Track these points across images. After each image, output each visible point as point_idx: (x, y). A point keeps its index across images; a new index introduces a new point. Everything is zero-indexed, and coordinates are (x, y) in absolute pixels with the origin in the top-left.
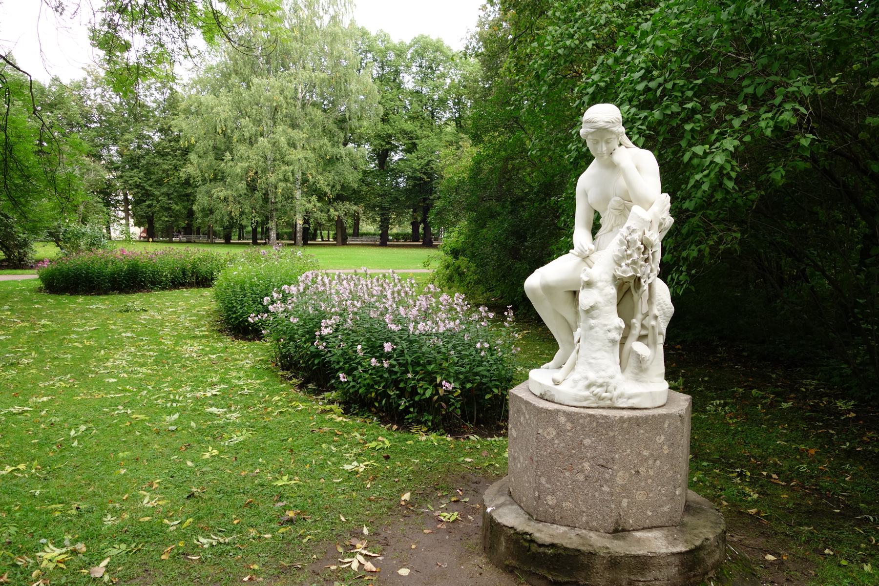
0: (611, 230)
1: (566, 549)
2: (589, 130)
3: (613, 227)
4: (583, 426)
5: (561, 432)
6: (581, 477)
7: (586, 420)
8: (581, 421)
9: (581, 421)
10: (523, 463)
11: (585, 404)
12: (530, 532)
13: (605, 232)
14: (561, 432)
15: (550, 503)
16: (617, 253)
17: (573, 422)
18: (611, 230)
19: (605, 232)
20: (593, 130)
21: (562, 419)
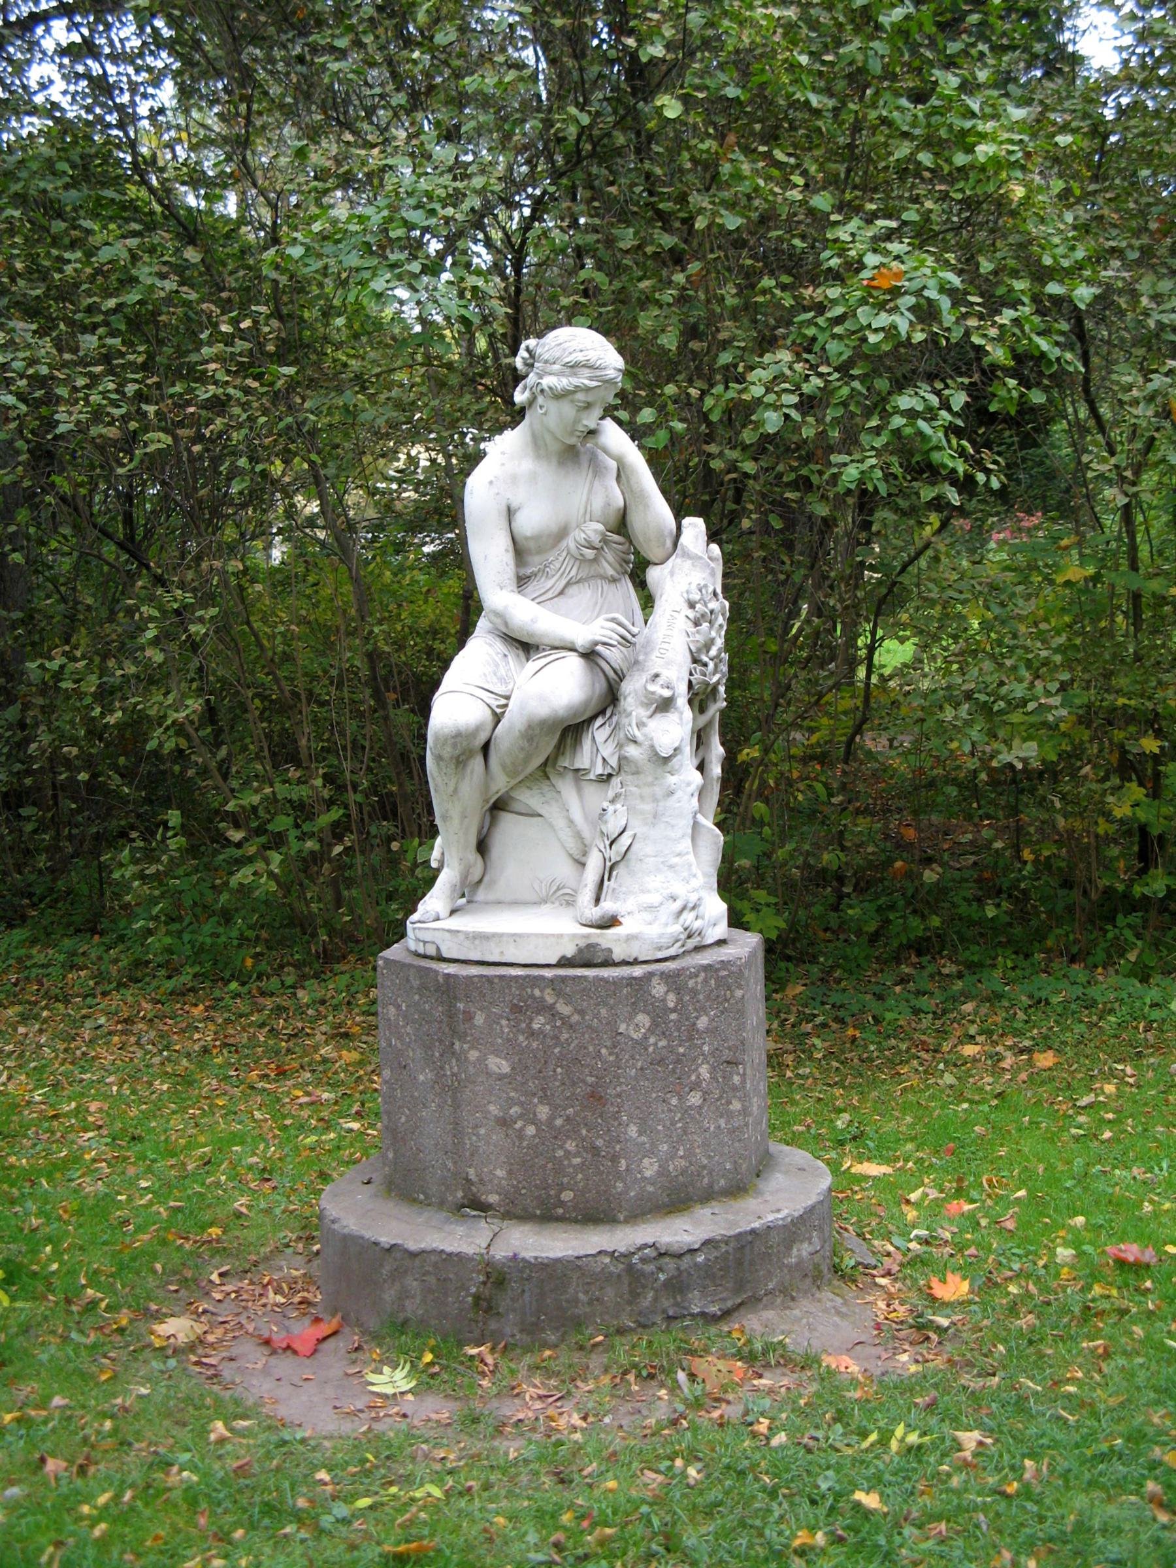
0: (561, 593)
1: (727, 1240)
2: (587, 382)
3: (568, 584)
4: (694, 992)
5: (659, 1015)
6: (695, 1099)
7: (700, 979)
8: (691, 983)
9: (691, 983)
10: (551, 1119)
11: (672, 952)
12: (650, 1241)
13: (549, 595)
14: (659, 1015)
15: (648, 1174)
17: (678, 991)
18: (561, 593)
19: (549, 595)
20: (594, 384)
21: (658, 989)
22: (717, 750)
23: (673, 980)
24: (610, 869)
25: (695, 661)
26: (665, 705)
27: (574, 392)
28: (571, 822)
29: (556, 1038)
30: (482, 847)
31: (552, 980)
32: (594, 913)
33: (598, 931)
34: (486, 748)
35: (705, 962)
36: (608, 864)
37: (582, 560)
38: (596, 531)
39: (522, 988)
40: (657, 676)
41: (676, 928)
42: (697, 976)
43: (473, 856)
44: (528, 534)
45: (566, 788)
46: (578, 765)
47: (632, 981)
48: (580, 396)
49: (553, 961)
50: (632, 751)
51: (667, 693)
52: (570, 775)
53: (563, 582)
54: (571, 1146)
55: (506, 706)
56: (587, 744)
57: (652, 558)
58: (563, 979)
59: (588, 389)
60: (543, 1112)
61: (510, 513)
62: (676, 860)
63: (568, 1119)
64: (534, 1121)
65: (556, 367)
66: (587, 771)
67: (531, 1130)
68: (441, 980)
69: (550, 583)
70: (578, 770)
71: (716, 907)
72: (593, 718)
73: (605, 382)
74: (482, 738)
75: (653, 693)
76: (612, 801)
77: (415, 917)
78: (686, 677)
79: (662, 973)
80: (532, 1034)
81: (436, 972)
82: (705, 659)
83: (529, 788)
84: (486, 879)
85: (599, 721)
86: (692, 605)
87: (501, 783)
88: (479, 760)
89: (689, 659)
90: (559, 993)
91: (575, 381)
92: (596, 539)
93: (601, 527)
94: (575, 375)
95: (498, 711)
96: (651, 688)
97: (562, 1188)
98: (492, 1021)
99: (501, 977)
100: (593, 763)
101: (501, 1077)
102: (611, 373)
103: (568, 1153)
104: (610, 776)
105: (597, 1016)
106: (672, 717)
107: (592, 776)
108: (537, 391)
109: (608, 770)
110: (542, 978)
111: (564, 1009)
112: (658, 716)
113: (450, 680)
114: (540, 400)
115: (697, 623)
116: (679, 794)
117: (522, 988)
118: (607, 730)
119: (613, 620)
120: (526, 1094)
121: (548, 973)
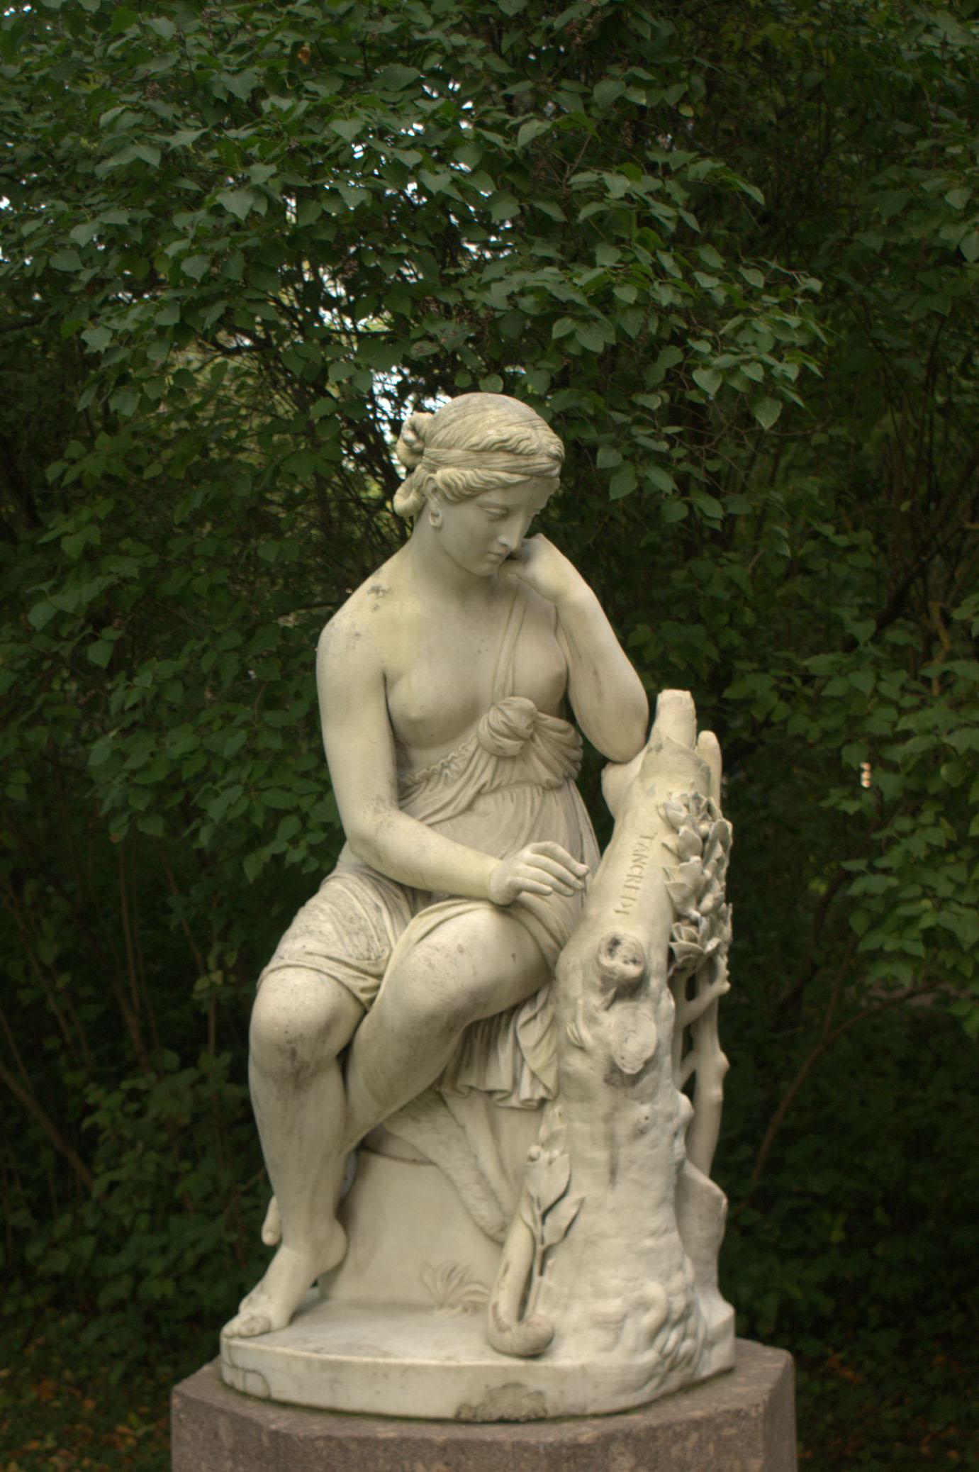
0: (470, 807)
2: (503, 475)
3: (479, 793)
8: (675, 1451)
13: (448, 812)
16: (679, 879)
18: (470, 807)
19: (448, 812)
20: (517, 478)
22: (714, 1061)
23: (641, 1443)
24: (542, 1256)
25: (679, 917)
26: (630, 990)
27: (484, 491)
28: (481, 1176)
30: (344, 1212)
31: (444, 1448)
32: (516, 1336)
33: (520, 1363)
34: (344, 1057)
35: (698, 1414)
36: (540, 1248)
37: (501, 757)
38: (522, 711)
40: (615, 942)
41: (649, 1357)
42: (686, 1438)
43: (327, 1227)
44: (415, 714)
45: (471, 1118)
46: (492, 1084)
47: (575, 1450)
48: (495, 498)
49: (449, 1412)
50: (576, 1062)
51: (633, 971)
52: (480, 1103)
53: (471, 791)
55: (377, 988)
56: (505, 1054)
58: (462, 1447)
59: (506, 486)
61: (386, 682)
62: (649, 1243)
65: (456, 453)
66: (508, 1095)
68: (265, 1440)
69: (449, 794)
70: (491, 1093)
71: (718, 1312)
72: (515, 1009)
73: (531, 475)
74: (336, 1042)
75: (611, 971)
76: (546, 1144)
77: (235, 1325)
78: (665, 942)
79: (627, 1436)
81: (259, 1427)
82: (695, 914)
83: (416, 1119)
84: (349, 1264)
85: (525, 1015)
86: (673, 827)
87: (366, 1117)
88: (331, 1079)
89: (670, 917)
91: (484, 474)
92: (522, 723)
93: (529, 704)
94: (482, 464)
95: (364, 997)
96: (606, 961)
99: (362, 1442)
100: (516, 1082)
102: (543, 462)
104: (543, 1101)
106: (645, 1009)
107: (514, 1102)
109: (540, 1093)
110: (428, 1443)
112: (618, 1007)
113: (293, 944)
114: (434, 503)
115: (681, 857)
116: (653, 1134)
118: (536, 1029)
119: (543, 852)
121: (438, 1435)
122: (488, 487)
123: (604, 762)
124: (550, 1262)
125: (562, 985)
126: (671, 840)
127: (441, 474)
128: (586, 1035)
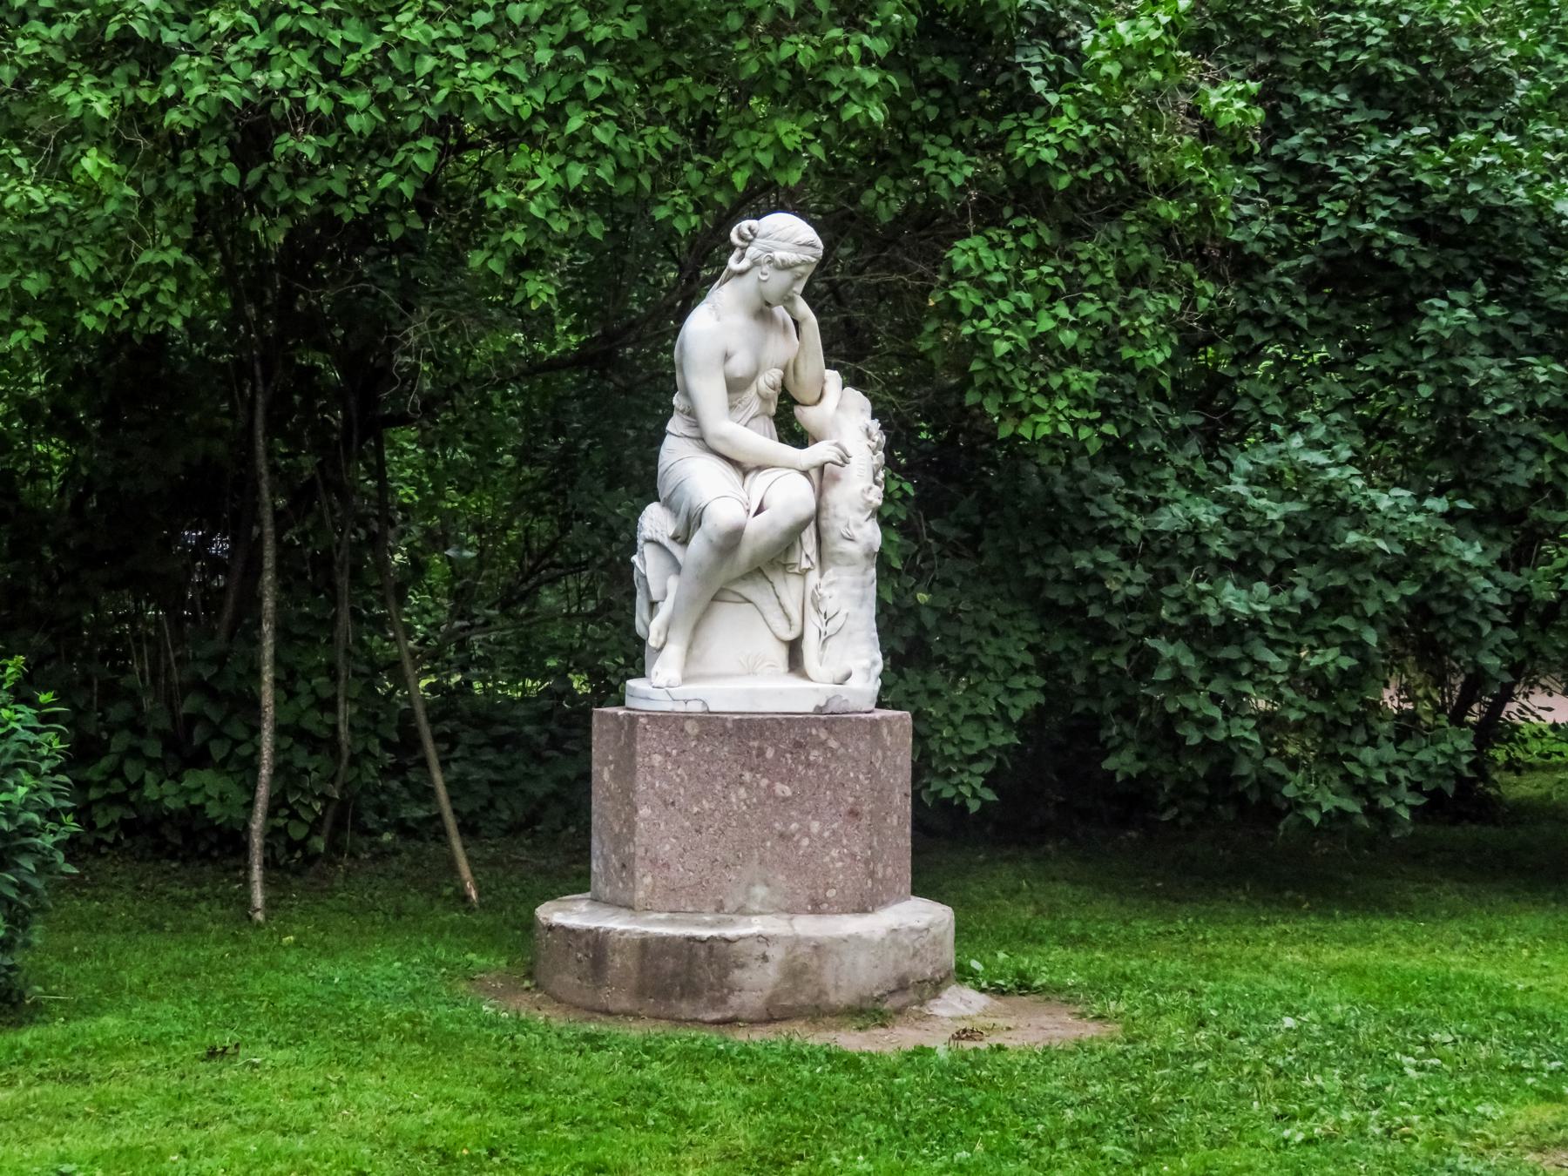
27: (797, 265)
29: (826, 767)
30: (696, 628)
39: (803, 728)
48: (801, 269)
54: (835, 853)
57: (808, 398)
58: (833, 721)
60: (815, 826)
61: (727, 357)
63: (834, 832)
64: (808, 835)
67: (805, 842)
68: (729, 725)
80: (809, 765)
86: (869, 436)
90: (830, 731)
91: (803, 257)
96: (870, 498)
97: (828, 887)
98: (780, 754)
101: (785, 799)
103: (833, 860)
105: (857, 749)
108: (764, 258)
111: (833, 744)
117: (803, 728)
120: (802, 812)
122: (804, 263)
123: (795, 402)
124: (829, 643)
125: (831, 511)
126: (873, 444)
127: (778, 255)
128: (856, 533)
